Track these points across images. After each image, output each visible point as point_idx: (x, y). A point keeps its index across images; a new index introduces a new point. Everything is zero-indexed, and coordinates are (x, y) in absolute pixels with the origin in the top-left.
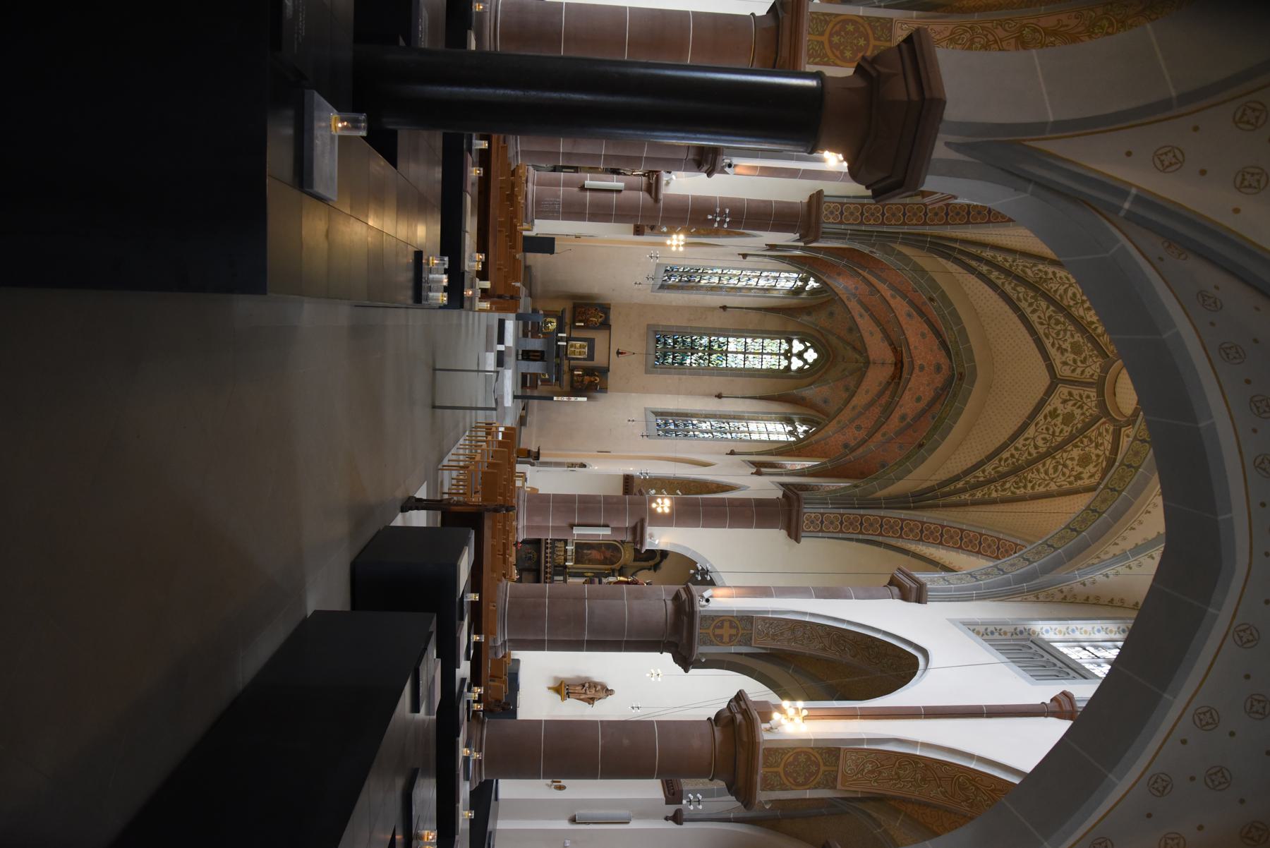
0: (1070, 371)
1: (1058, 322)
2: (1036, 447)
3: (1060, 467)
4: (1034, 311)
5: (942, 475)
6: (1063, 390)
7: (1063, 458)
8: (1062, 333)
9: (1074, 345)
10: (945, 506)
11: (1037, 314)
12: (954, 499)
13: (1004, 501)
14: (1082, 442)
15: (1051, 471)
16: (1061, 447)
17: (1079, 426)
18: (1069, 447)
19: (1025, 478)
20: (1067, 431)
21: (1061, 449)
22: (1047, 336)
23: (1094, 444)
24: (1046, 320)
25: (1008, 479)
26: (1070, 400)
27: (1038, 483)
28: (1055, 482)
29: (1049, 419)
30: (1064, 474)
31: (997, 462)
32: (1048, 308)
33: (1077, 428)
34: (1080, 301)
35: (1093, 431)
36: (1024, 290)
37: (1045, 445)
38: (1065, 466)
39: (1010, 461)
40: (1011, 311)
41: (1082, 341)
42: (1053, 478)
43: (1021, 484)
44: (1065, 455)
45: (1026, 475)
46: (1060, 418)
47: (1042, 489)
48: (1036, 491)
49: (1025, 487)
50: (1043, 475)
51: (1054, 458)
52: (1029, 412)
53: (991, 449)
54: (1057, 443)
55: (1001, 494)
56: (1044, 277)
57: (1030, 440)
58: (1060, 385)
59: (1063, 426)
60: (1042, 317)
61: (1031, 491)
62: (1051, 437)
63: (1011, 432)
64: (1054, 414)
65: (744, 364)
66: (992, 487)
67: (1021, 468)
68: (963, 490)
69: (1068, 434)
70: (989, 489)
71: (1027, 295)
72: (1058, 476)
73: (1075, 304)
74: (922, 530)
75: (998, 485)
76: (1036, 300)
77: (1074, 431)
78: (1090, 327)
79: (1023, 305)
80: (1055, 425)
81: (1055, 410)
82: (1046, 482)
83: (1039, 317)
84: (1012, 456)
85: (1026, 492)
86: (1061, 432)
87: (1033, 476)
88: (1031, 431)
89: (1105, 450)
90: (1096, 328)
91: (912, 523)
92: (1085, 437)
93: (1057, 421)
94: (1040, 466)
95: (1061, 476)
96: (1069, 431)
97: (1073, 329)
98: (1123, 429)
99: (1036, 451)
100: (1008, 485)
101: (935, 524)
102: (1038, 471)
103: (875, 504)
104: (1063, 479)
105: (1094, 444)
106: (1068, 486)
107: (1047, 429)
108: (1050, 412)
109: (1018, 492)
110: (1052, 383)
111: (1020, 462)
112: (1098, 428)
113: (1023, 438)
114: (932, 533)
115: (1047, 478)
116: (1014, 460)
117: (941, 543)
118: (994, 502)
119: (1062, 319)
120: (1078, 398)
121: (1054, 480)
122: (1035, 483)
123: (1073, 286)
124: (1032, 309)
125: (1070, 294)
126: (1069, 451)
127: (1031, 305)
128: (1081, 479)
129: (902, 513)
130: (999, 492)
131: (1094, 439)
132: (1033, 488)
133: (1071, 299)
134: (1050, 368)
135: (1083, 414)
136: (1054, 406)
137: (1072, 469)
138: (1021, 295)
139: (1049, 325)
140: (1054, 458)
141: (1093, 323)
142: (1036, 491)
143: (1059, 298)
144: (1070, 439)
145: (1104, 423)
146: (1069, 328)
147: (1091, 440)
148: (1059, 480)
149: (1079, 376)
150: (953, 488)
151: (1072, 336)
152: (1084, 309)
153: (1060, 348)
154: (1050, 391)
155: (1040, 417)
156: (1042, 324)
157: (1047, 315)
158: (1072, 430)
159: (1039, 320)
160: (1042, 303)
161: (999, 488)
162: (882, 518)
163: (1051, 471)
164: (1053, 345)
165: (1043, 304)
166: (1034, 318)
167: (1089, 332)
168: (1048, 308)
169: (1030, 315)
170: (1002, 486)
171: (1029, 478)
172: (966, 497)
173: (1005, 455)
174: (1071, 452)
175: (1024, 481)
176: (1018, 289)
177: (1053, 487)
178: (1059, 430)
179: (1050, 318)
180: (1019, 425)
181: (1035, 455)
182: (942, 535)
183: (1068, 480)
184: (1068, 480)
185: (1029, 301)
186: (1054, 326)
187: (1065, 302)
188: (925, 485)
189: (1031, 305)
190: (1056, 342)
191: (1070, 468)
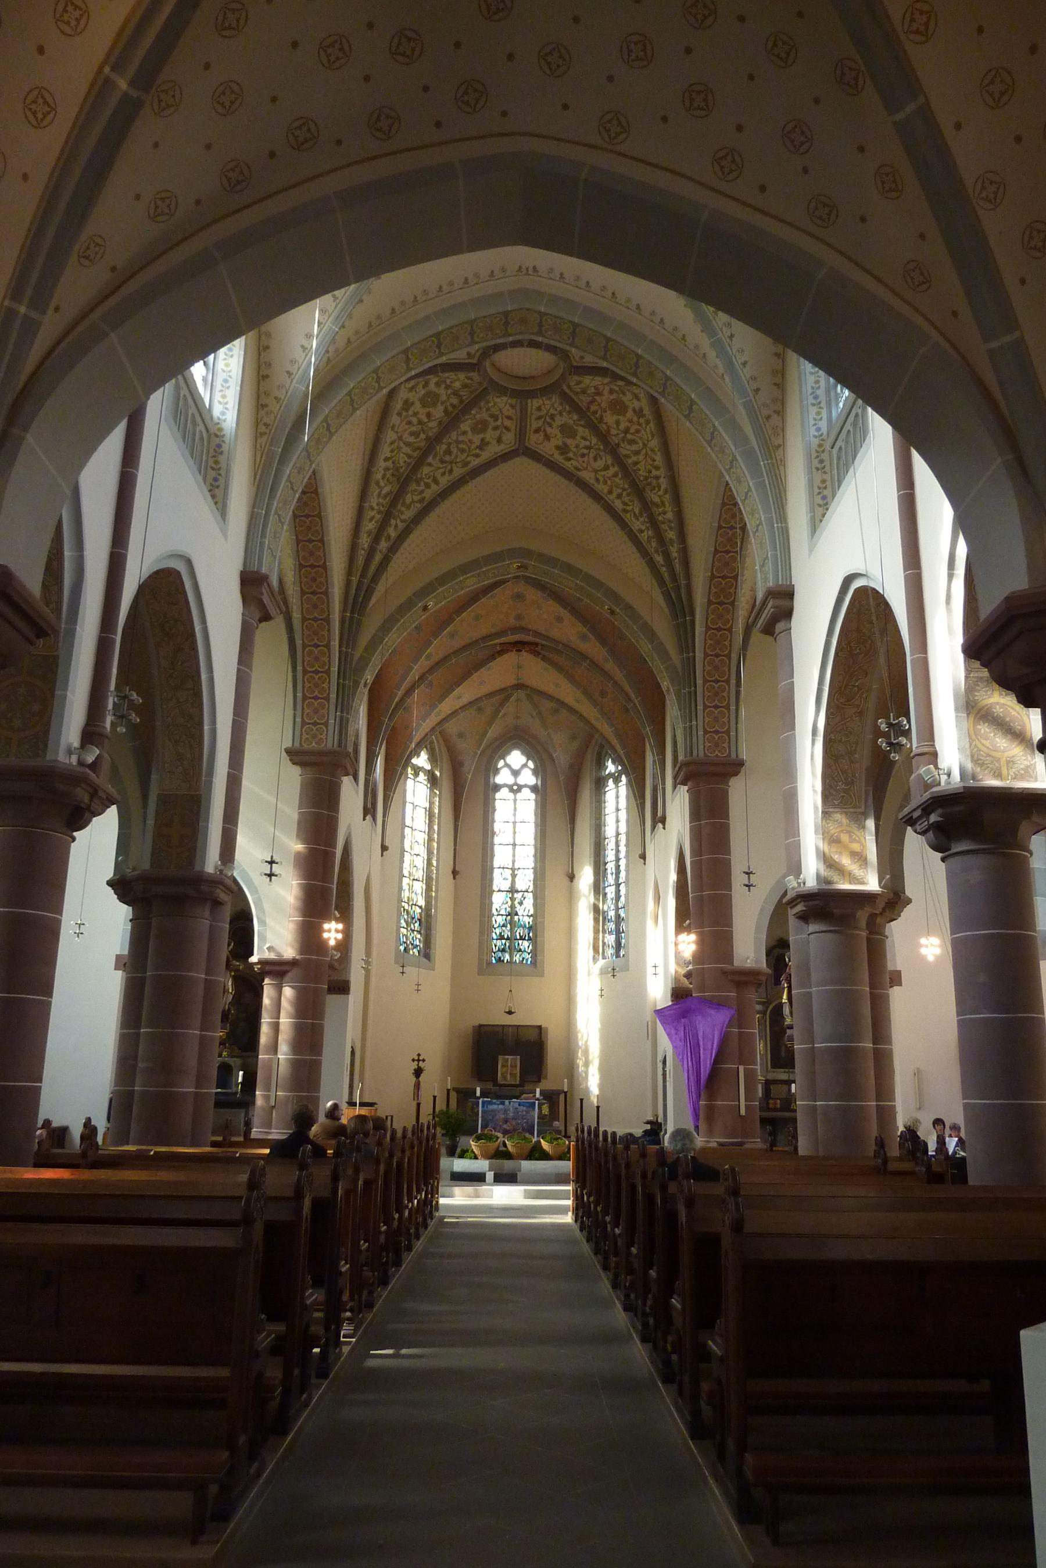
1: (448, 452)
2: (606, 468)
3: (629, 436)
4: (436, 482)
6: (534, 440)
7: (618, 434)
8: (461, 446)
9: (475, 430)
11: (439, 476)
13: (677, 500)
15: (634, 448)
16: (603, 437)
19: (646, 478)
24: (446, 467)
29: (571, 455)
30: (638, 431)
31: (628, 515)
32: (430, 465)
33: (579, 420)
34: (420, 427)
36: (409, 495)
37: (604, 458)
38: (626, 431)
39: (626, 499)
41: (470, 421)
44: (613, 432)
45: (642, 478)
46: (569, 441)
49: (657, 478)
50: (641, 457)
51: (618, 445)
54: (599, 443)
58: (527, 444)
61: (662, 469)
62: (592, 450)
64: (563, 449)
67: (634, 484)
68: (667, 555)
69: (587, 430)
71: (416, 490)
72: (641, 438)
73: (424, 433)
75: (656, 511)
76: (421, 479)
77: (582, 423)
79: (428, 494)
80: (577, 447)
81: (558, 448)
82: (649, 452)
83: (443, 474)
84: (619, 496)
85: (663, 476)
86: (585, 439)
87: (643, 468)
88: (587, 476)
92: (588, 408)
94: (630, 461)
95: (640, 435)
98: (575, 364)
99: (611, 468)
100: (656, 499)
102: (636, 463)
105: (597, 398)
107: (583, 455)
108: (562, 454)
109: (663, 486)
115: (644, 451)
116: (624, 494)
119: (444, 447)
121: (646, 442)
122: (652, 465)
125: (412, 439)
127: (428, 486)
128: (641, 410)
130: (666, 509)
131: (591, 398)
132: (657, 468)
134: (506, 457)
135: (561, 414)
137: (631, 421)
138: (416, 498)
139: (451, 462)
140: (618, 445)
145: (569, 387)
147: (593, 401)
151: (465, 433)
155: (568, 465)
156: (451, 471)
158: (582, 426)
163: (634, 448)
164: (477, 456)
165: (426, 470)
166: (444, 481)
168: (430, 465)
169: (441, 486)
170: (657, 506)
173: (618, 505)
175: (650, 480)
177: (654, 443)
178: (582, 441)
179: (442, 461)
181: (616, 468)
189: (428, 486)
190: (474, 452)
191: (629, 425)
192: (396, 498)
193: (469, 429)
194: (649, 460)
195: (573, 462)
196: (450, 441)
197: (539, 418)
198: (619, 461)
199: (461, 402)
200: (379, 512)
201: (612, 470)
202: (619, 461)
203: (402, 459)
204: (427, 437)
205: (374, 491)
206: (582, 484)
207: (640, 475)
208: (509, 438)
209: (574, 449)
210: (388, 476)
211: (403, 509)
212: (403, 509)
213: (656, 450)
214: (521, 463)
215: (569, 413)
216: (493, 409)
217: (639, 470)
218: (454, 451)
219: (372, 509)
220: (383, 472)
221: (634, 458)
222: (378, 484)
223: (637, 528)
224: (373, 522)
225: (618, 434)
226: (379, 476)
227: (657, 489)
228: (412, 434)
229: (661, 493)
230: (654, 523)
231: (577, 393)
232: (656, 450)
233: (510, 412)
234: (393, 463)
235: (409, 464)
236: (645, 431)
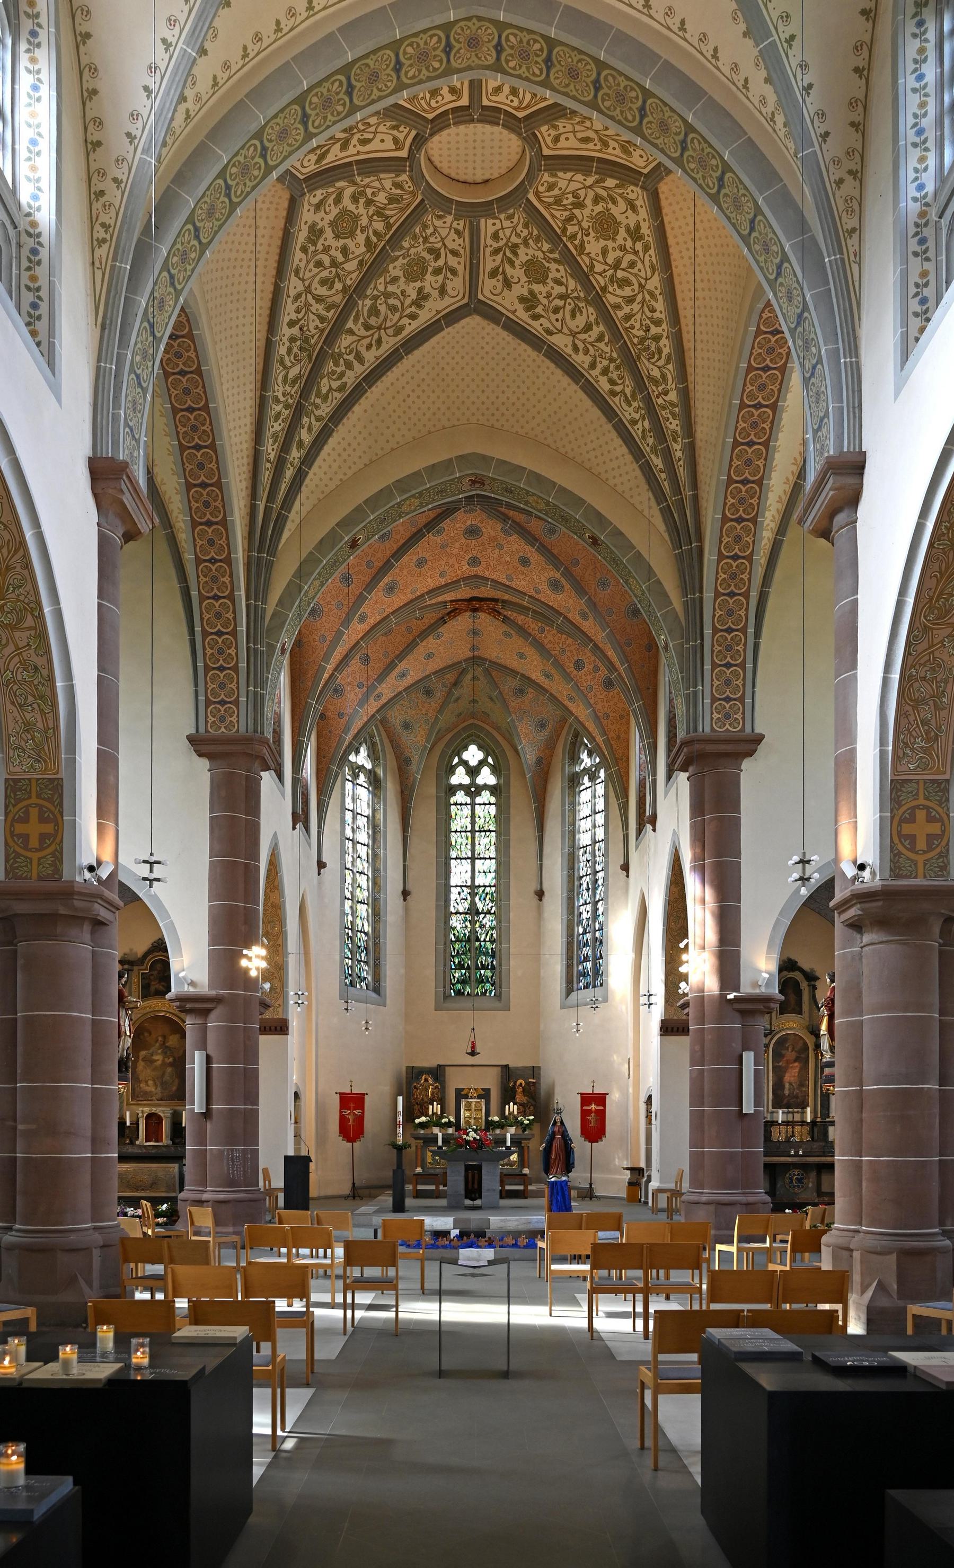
0: (455, 279)
1: (374, 311)
2: (588, 328)
3: (620, 274)
4: (360, 359)
5: (643, 497)
6: (488, 288)
7: (605, 271)
10: (695, 485)
11: (363, 350)
12: (682, 471)
13: (682, 374)
14: (574, 236)
15: (627, 291)
16: (583, 277)
17: (546, 247)
18: (584, 261)
19: (642, 340)
20: (558, 270)
21: (588, 277)
22: (399, 330)
23: (577, 212)
24: (372, 335)
25: (644, 373)
26: (504, 272)
27: (649, 315)
28: (646, 279)
29: (539, 310)
30: (632, 265)
31: (617, 399)
32: (351, 332)
33: (551, 251)
34: (334, 270)
35: (553, 216)
36: (325, 381)
37: (584, 310)
38: (616, 265)
40: (362, 400)
41: (401, 261)
42: (640, 284)
43: (653, 349)
44: (599, 268)
45: (635, 340)
46: (536, 288)
47: (660, 305)
48: (663, 316)
49: (657, 338)
50: (636, 307)
51: (604, 289)
52: (529, 350)
53: (596, 413)
54: (579, 288)
55: (671, 385)
56: (298, 343)
57: (577, 341)
58: (480, 297)
59: (549, 281)
60: (367, 341)
61: (664, 326)
62: (569, 300)
63: (566, 381)
64: (529, 302)
65: (490, 858)
66: (660, 401)
67: (625, 350)
68: (667, 455)
69: (561, 268)
70: (664, 408)
71: (334, 373)
72: (636, 275)
73: (340, 280)
74: (736, 520)
75: (654, 390)
76: (340, 355)
80: (548, 296)
81: (522, 299)
82: (647, 297)
83: (369, 347)
84: (605, 371)
85: (665, 334)
86: (558, 282)
87: (637, 325)
88: (561, 342)
89: (586, 187)
90: (376, 233)
91: (726, 540)
92: (564, 230)
93: (541, 293)
94: (620, 314)
95: (635, 271)
96: (556, 266)
97: (382, 280)
99: (594, 327)
100: (656, 373)
101: (726, 498)
102: (628, 317)
103: (695, 609)
104: (640, 265)
105: (577, 212)
106: (652, 252)
107: (556, 310)
108: (527, 309)
109: (666, 351)
110: (476, 311)
111: (615, 355)
112: (548, 206)
113: (574, 356)
114: (742, 501)
116: (612, 365)
117: (760, 483)
118: (685, 395)
119: (368, 302)
120: (499, 257)
121: (643, 282)
122: (650, 319)
123: (309, 286)
124: (355, 362)
125: (323, 291)
126: (591, 259)
127: (349, 366)
128: (638, 227)
129: (709, 559)
130: (669, 387)
131: (567, 213)
132: (658, 323)
133: (331, 288)
134: (452, 317)
135: (526, 243)
136: (516, 301)
137: (622, 248)
138: (335, 385)
139: (379, 328)
141: (368, 239)
142: (663, 316)
143: (333, 311)
144: (569, 260)
145: (537, 194)
146: (381, 288)
147: (569, 219)
148: (643, 274)
149: (462, 260)
150: (663, 476)
151: (395, 280)
152: (347, 260)
153: (417, 303)
154: (491, 314)
155: (536, 327)
156: (379, 342)
157: (363, 332)
158: (555, 260)
159: (374, 348)
160: (345, 343)
161: (660, 389)
162: (717, 594)
163: (627, 291)
164: (413, 317)
165: (345, 341)
166: (371, 357)
167: (384, 247)
168: (351, 332)
169: (367, 365)
170: (656, 383)
171: (641, 333)
172: (677, 450)
173: (604, 385)
174: (593, 255)
175: (646, 343)
176: (324, 390)
177: (655, 283)
178: (555, 286)
179: (367, 327)
180: (552, 366)
181: (602, 328)
182: (744, 482)
183: (641, 254)
184: (641, 254)
185: (343, 368)
186: (382, 318)
187: (338, 299)
188: (662, 527)
189: (349, 366)
190: (408, 311)
191: (621, 254)
192: (309, 384)
193: (400, 274)
194: (646, 309)
195: (542, 320)
196: (375, 292)
197: (496, 252)
198: (605, 315)
199: (389, 226)
200: (287, 407)
201: (596, 331)
202: (605, 315)
204: (344, 287)
205: (278, 373)
206: (555, 355)
207: (635, 336)
208: (457, 285)
209: (545, 301)
210: (295, 350)
211: (318, 401)
212: (318, 401)
213: (657, 292)
215: (537, 240)
216: (432, 240)
217: (633, 328)
218: (382, 309)
219: (277, 401)
220: (287, 344)
221: (627, 310)
222: (282, 362)
223: (629, 418)
224: (280, 421)
225: (605, 271)
226: (283, 351)
227: (656, 356)
228: (323, 282)
229: (661, 363)
230: (651, 409)
231: (550, 204)
232: (657, 292)
234: (301, 329)
235: (322, 331)
236: (643, 262)
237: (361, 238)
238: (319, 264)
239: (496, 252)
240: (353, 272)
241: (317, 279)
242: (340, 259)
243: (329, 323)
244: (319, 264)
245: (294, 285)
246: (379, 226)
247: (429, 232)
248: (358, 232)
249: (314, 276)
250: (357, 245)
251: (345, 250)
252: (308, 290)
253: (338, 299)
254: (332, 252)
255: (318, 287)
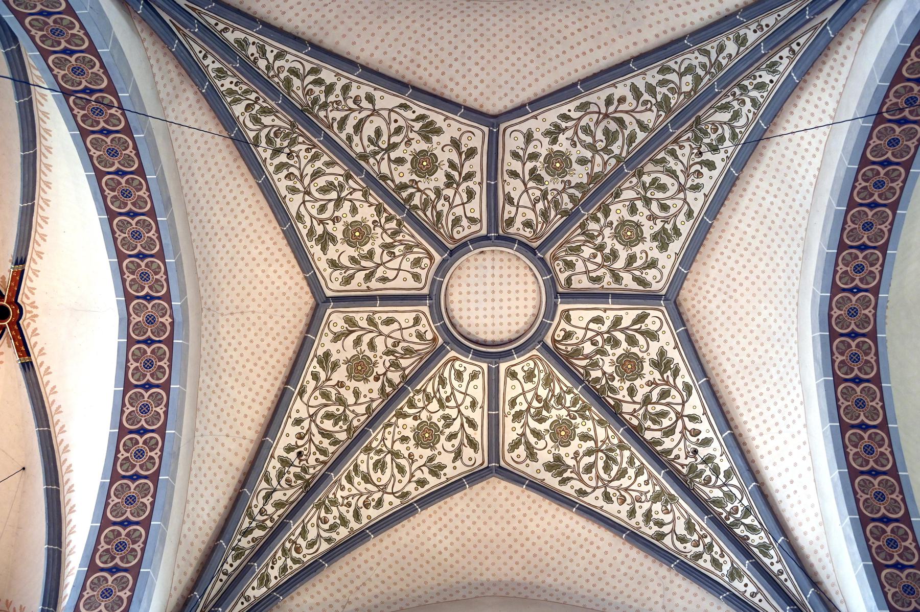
34: (648, 195)
73: (644, 184)
78: (599, 209)
90: (597, 220)
123: (679, 191)
125: (665, 179)
133: (655, 180)
143: (659, 157)
152: (632, 201)
197: (470, 176)
203: (685, 153)
204: (640, 176)
214: (495, 104)
228: (663, 188)
233: (514, 187)
237: (614, 217)
238: (664, 208)
239: (470, 176)
240: (627, 188)
241: (668, 194)
242: (639, 204)
243: (665, 148)
244: (664, 208)
245: (697, 202)
246: (592, 226)
247: (540, 206)
248: (615, 224)
249: (672, 198)
250: (619, 211)
251: (633, 210)
252: (682, 188)
253: (650, 167)
254: (647, 213)
255: (669, 186)
